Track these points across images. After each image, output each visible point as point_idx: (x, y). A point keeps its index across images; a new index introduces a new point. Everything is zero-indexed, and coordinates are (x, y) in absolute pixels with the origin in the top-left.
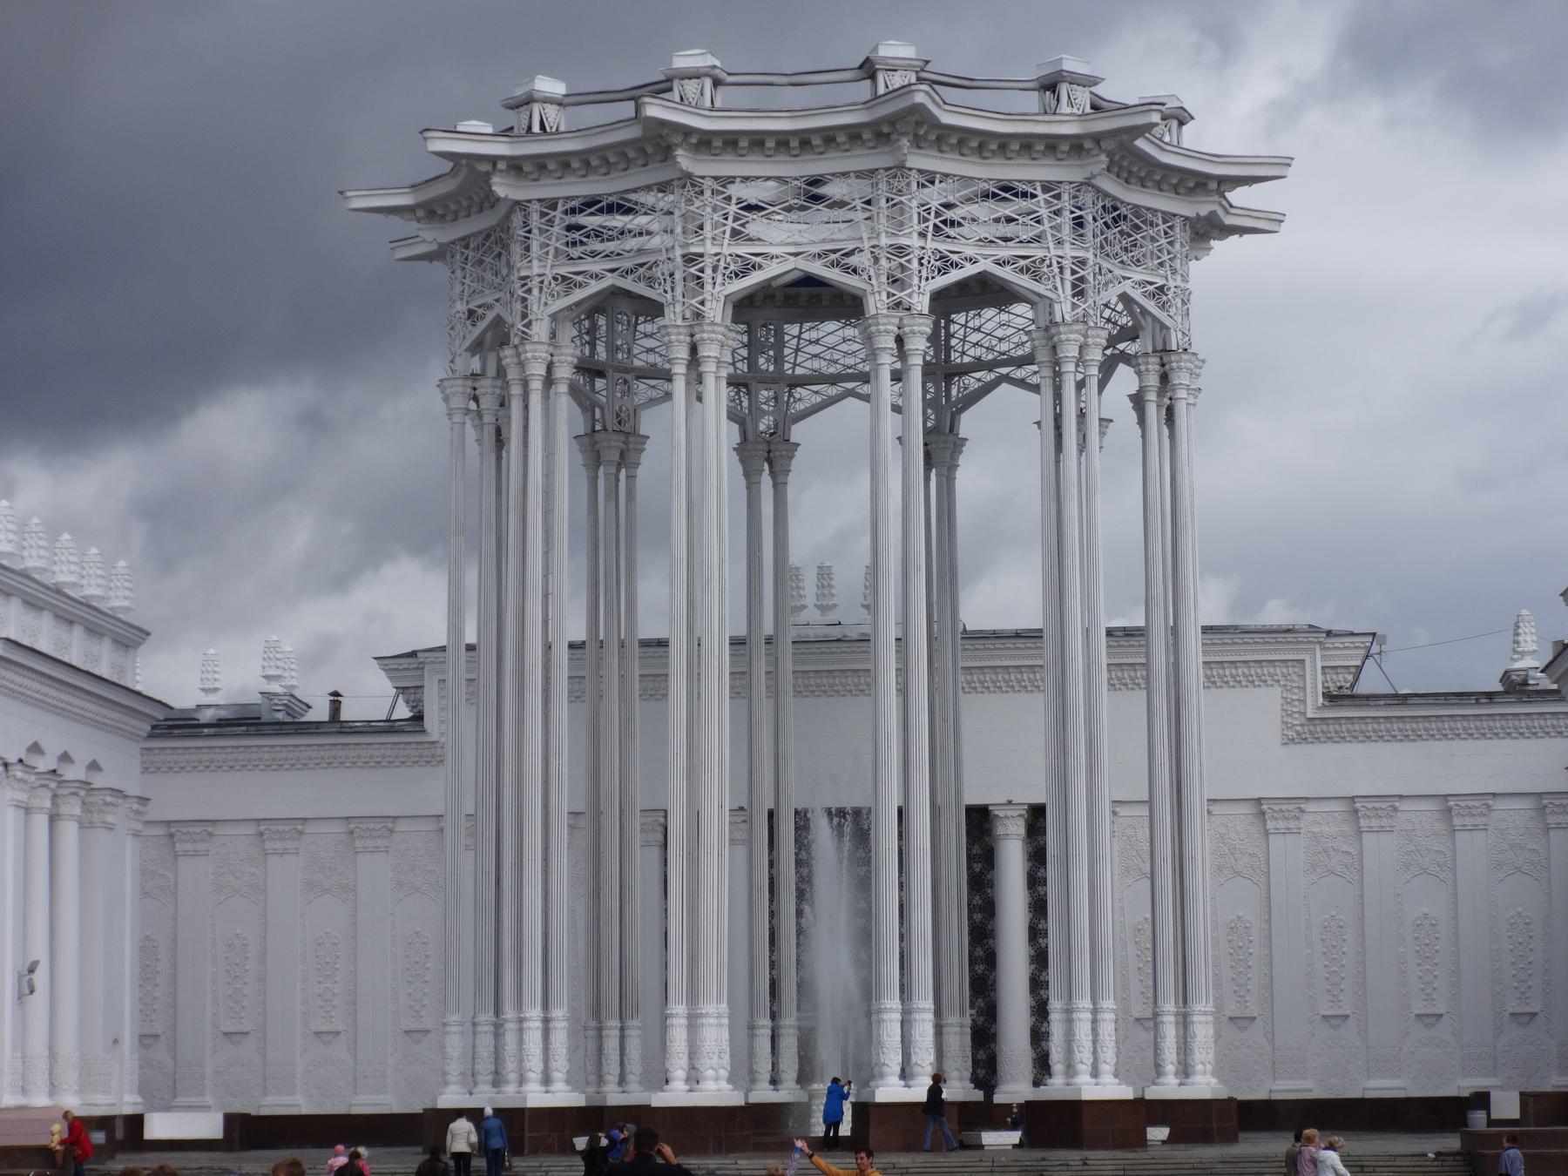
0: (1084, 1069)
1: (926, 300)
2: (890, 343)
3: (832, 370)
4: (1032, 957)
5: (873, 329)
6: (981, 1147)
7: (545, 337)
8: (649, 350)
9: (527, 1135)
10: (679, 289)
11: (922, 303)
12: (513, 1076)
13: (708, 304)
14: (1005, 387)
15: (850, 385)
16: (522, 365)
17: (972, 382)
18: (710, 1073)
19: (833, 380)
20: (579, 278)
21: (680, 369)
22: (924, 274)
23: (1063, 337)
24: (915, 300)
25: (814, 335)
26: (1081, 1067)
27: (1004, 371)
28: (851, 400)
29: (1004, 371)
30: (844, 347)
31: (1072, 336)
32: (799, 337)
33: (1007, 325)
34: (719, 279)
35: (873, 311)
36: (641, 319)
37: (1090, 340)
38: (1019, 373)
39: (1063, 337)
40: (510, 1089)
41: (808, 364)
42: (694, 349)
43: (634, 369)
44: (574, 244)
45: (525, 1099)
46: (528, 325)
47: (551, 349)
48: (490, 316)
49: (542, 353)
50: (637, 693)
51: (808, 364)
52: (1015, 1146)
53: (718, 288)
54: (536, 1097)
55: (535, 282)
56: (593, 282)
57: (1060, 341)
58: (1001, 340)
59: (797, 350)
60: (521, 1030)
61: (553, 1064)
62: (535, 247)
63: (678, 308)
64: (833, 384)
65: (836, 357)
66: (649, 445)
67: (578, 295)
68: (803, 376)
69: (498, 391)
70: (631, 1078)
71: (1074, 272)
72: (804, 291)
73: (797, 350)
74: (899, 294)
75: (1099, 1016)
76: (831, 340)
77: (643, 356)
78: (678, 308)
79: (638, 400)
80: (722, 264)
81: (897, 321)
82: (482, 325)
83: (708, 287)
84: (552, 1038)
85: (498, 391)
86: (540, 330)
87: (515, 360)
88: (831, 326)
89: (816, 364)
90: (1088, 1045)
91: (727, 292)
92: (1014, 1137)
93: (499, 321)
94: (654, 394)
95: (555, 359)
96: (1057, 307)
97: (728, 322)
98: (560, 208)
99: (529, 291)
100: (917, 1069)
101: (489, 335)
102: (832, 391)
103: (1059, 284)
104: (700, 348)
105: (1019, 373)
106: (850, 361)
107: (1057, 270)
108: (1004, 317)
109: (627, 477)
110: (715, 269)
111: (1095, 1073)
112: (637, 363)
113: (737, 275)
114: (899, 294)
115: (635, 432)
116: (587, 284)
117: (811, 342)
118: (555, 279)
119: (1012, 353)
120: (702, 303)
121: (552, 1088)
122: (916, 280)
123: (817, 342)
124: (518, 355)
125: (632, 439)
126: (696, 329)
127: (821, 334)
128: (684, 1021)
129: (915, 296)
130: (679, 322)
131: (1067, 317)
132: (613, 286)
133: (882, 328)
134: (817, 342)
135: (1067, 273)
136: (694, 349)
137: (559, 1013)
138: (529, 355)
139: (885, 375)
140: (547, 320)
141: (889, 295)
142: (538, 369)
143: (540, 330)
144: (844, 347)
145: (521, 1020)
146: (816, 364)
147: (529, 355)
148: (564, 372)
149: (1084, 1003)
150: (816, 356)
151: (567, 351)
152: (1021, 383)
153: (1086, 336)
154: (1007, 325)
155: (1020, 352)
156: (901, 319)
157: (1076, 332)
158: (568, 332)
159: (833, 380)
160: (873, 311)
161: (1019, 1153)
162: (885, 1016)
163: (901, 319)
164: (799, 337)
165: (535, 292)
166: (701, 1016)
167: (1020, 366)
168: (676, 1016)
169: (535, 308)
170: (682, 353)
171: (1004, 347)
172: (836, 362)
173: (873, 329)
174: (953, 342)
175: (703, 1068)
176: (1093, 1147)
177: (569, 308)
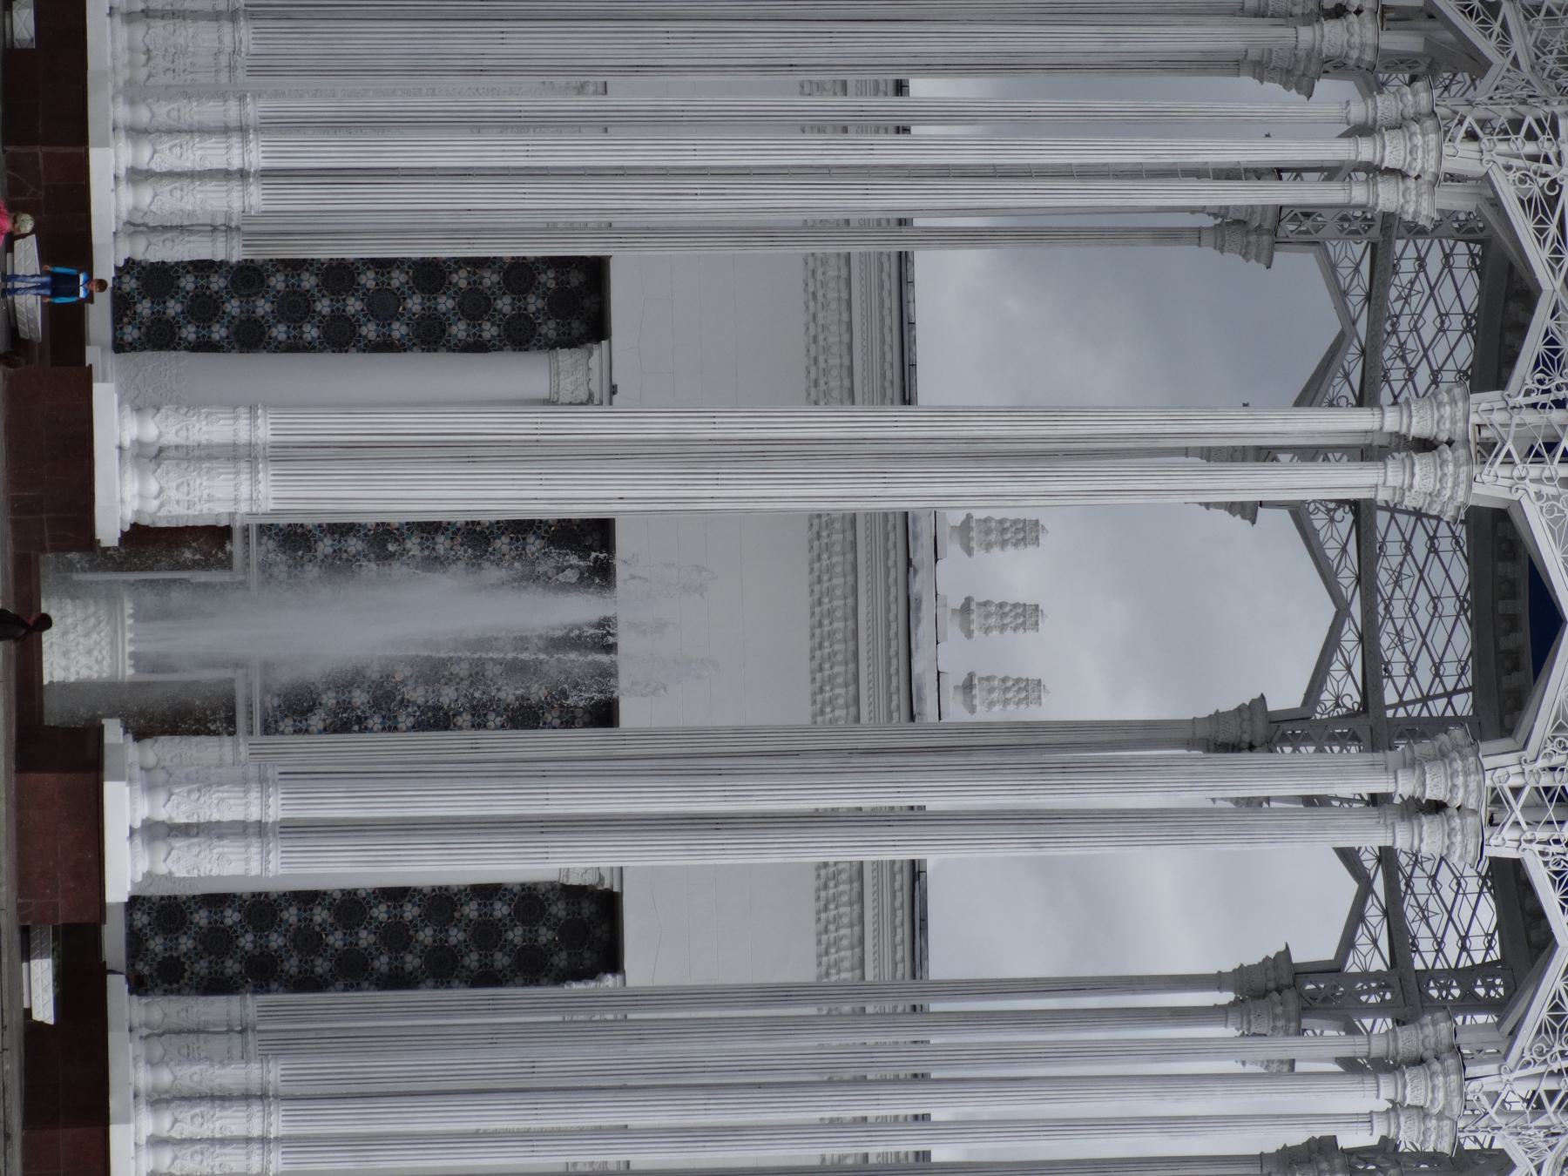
0: (164, 1123)
1: (1509, 852)
2: (1433, 793)
3: (1383, 577)
4: (355, 892)
5: (1458, 765)
6: (27, 955)
7: (1449, 165)
8: (1421, 262)
9: (40, 151)
10: (1531, 417)
11: (1503, 845)
12: (143, 116)
13: (1505, 471)
14: (1352, 887)
15: (1356, 609)
16: (1399, 125)
18: (153, 487)
20: (1553, 229)
21: (1392, 421)
22: (1554, 848)
23: (1440, 1080)
24: (1509, 833)
25: (1445, 544)
26: (166, 1120)
27: (1379, 885)
28: (1331, 610)
29: (1379, 885)
31: (1440, 1095)
33: (1459, 890)
34: (1548, 490)
35: (1488, 762)
36: (1477, 249)
37: (1432, 1123)
38: (1374, 913)
39: (1440, 1080)
40: (122, 113)
41: (1394, 534)
42: (1426, 445)
43: (1389, 243)
45: (105, 144)
46: (1472, 136)
47: (1427, 177)
48: (1488, 47)
49: (1424, 162)
50: (818, 250)
51: (1394, 534)
52: (28, 1012)
53: (1532, 488)
54: (106, 162)
55: (1545, 146)
56: (1546, 253)
57: (1433, 1075)
58: (1433, 878)
60: (226, 130)
61: (165, 187)
63: (1499, 417)
64: (1359, 580)
65: (1406, 584)
66: (1257, 267)
67: (1523, 226)
68: (1373, 527)
69: (1354, 54)
70: (146, 195)
71: (1552, 1095)
72: (1522, 606)
74: (1517, 807)
75: (255, 1147)
76: (1436, 575)
77: (1411, 252)
78: (1499, 417)
79: (1336, 249)
81: (1472, 804)
82: (1470, 28)
83: (1535, 471)
84: (211, 142)
85: (1354, 54)
86: (1463, 157)
87: (1410, 112)
88: (1460, 574)
89: (1394, 549)
90: (206, 1131)
91: (1525, 503)
92: (44, 1012)
93: (1480, 66)
94: (1345, 272)
95: (1411, 183)
96: (1492, 1068)
97: (1472, 502)
99: (1531, 136)
100: (161, 849)
101: (1449, 36)
102: (1347, 579)
103: (1532, 1070)
104: (1437, 819)
106: (1399, 609)
107: (1555, 1067)
109: (1200, 230)
111: (157, 1142)
112: (1399, 245)
113: (1555, 521)
114: (1517, 807)
115: (1278, 242)
116: (1542, 243)
117: (1432, 539)
118: (1553, 183)
119: (1409, 900)
120: (1508, 460)
121: (123, 187)
122: (1543, 834)
123: (1433, 549)
124: (1417, 119)
125: (1266, 239)
126: (1462, 452)
127: (1446, 557)
128: (243, 436)
129: (1515, 834)
130: (1474, 419)
131: (1474, 1085)
132: (1540, 290)
133: (1460, 780)
134: (1433, 549)
135: (1551, 1085)
136: (1426, 445)
137: (256, 197)
138: (1418, 140)
139: (1380, 786)
140: (1480, 170)
141: (1516, 791)
142: (1393, 152)
143: (1463, 157)
144: (1423, 598)
145: (243, 130)
146: (1394, 549)
147: (1418, 140)
148: (1387, 197)
149: (278, 1125)
150: (1408, 548)
151: (1425, 204)
152: (1357, 916)
153: (1440, 1116)
154: (1459, 890)
155: (1411, 914)
156: (1475, 812)
157: (1448, 1103)
158: (1457, 200)
159: (1366, 580)
160: (1488, 762)
161: (18, 1018)
162: (254, 795)
163: (1475, 812)
165: (1531, 148)
166: (254, 472)
167: (1386, 913)
168: (254, 481)
169: (1503, 147)
170: (1420, 425)
171: (1421, 885)
172: (1397, 583)
173: (1458, 765)
175: (166, 447)
176: (28, 1147)
177: (1496, 203)
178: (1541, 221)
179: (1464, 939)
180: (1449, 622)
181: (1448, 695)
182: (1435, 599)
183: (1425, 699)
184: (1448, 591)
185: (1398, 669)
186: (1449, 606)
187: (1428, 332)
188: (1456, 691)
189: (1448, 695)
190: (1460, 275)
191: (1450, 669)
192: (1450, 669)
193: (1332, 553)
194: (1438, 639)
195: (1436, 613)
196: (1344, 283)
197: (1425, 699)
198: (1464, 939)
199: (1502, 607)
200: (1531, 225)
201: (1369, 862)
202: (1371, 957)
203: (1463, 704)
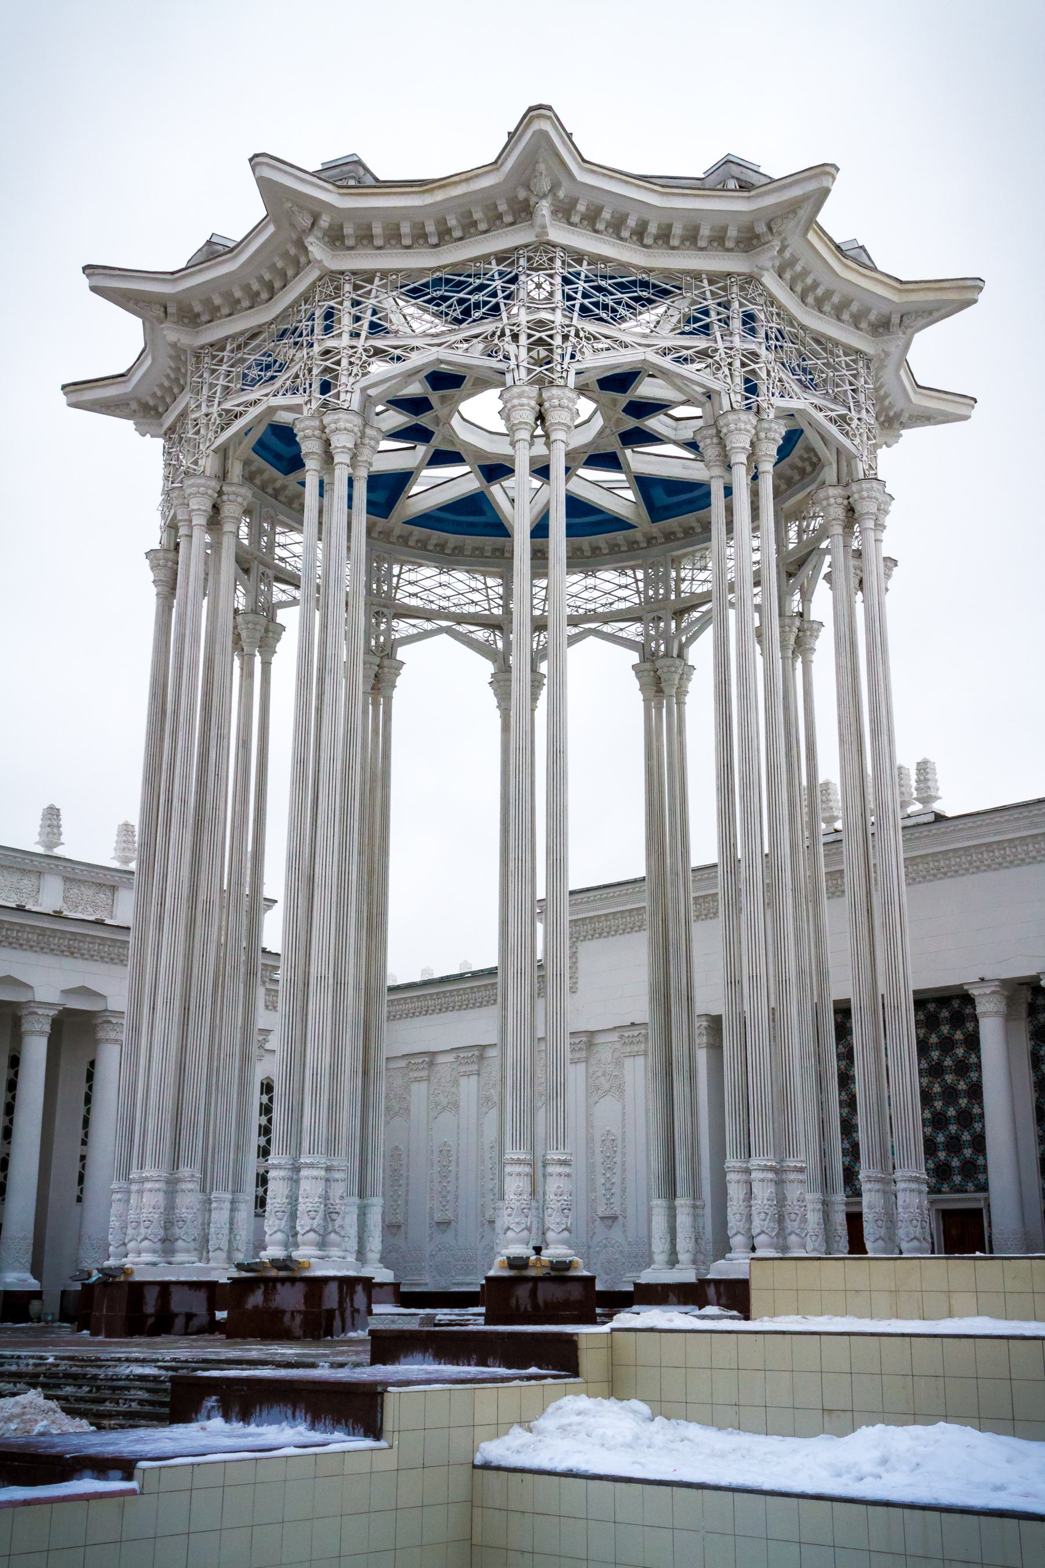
14: (591, 639)
19: (428, 615)
25: (412, 576)
38: (607, 629)
65: (431, 598)
76: (427, 584)
94: (284, 598)
105: (607, 629)
106: (444, 603)
108: (591, 581)
117: (410, 583)
144: (439, 591)
150: (415, 595)
159: (428, 615)
167: (606, 623)
172: (432, 602)
174: (535, 601)
179: (620, 587)
184: (437, 578)
185: (472, 609)
186: (444, 578)
189: (487, 588)
191: (473, 584)
192: (473, 584)
193: (415, 631)
196: (291, 599)
198: (620, 587)
201: (574, 631)
202: (633, 630)
203: (490, 582)
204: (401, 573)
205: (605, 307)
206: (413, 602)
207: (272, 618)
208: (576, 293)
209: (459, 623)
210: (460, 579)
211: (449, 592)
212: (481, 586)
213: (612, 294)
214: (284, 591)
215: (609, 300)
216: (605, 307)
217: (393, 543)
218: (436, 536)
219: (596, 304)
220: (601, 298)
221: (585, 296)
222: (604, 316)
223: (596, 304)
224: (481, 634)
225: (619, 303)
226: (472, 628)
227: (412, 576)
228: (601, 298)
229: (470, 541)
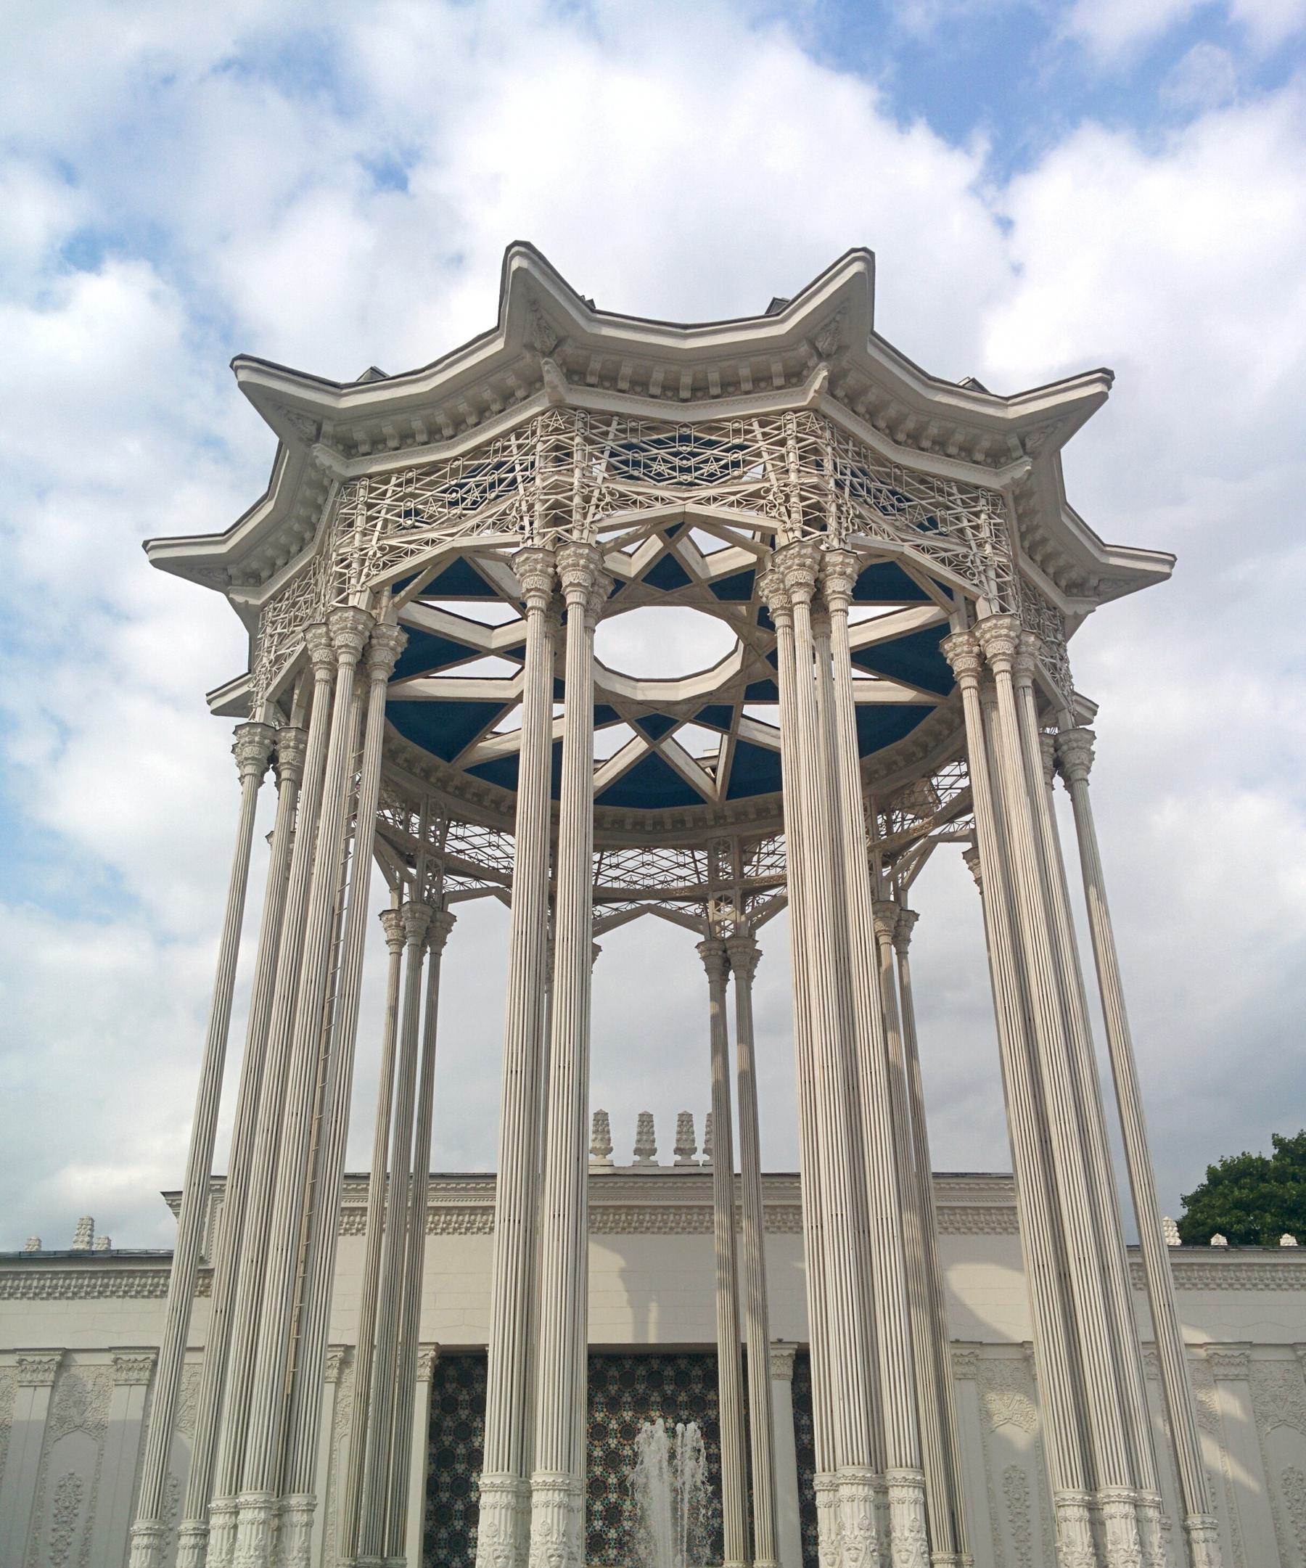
17: (764, 898)
25: (614, 860)
30: (642, 870)
32: (600, 862)
44: (408, 514)
59: (598, 873)
62: (360, 522)
73: (598, 873)
76: (630, 864)
80: (596, 494)
83: (576, 516)
98: (394, 481)
106: (649, 882)
110: (587, 499)
123: (617, 866)
127: (621, 860)
134: (617, 866)
144: (642, 870)
150: (616, 878)
164: (600, 862)
172: (635, 883)
178: (406, 554)
180: (656, 858)
181: (695, 861)
182: (643, 864)
183: (698, 873)
184: (639, 858)
186: (647, 857)
187: (498, 854)
188: (693, 857)
189: (695, 861)
190: (467, 833)
191: (681, 859)
192: (681, 859)
194: (666, 864)
195: (652, 864)
197: (698, 873)
199: (649, 828)
200: (408, 559)
203: (698, 855)
204: (602, 858)
205: (636, 464)
206: (616, 885)
207: (443, 909)
208: (602, 452)
209: (664, 901)
210: (665, 856)
211: (654, 870)
212: (689, 860)
213: (644, 450)
214: (462, 884)
215: (640, 456)
216: (636, 464)
217: (607, 829)
218: (630, 813)
219: (625, 463)
220: (630, 455)
221: (612, 455)
222: (636, 473)
223: (625, 463)
224: (693, 909)
225: (654, 459)
226: (681, 904)
227: (614, 860)
228: (630, 455)
229: (666, 813)
